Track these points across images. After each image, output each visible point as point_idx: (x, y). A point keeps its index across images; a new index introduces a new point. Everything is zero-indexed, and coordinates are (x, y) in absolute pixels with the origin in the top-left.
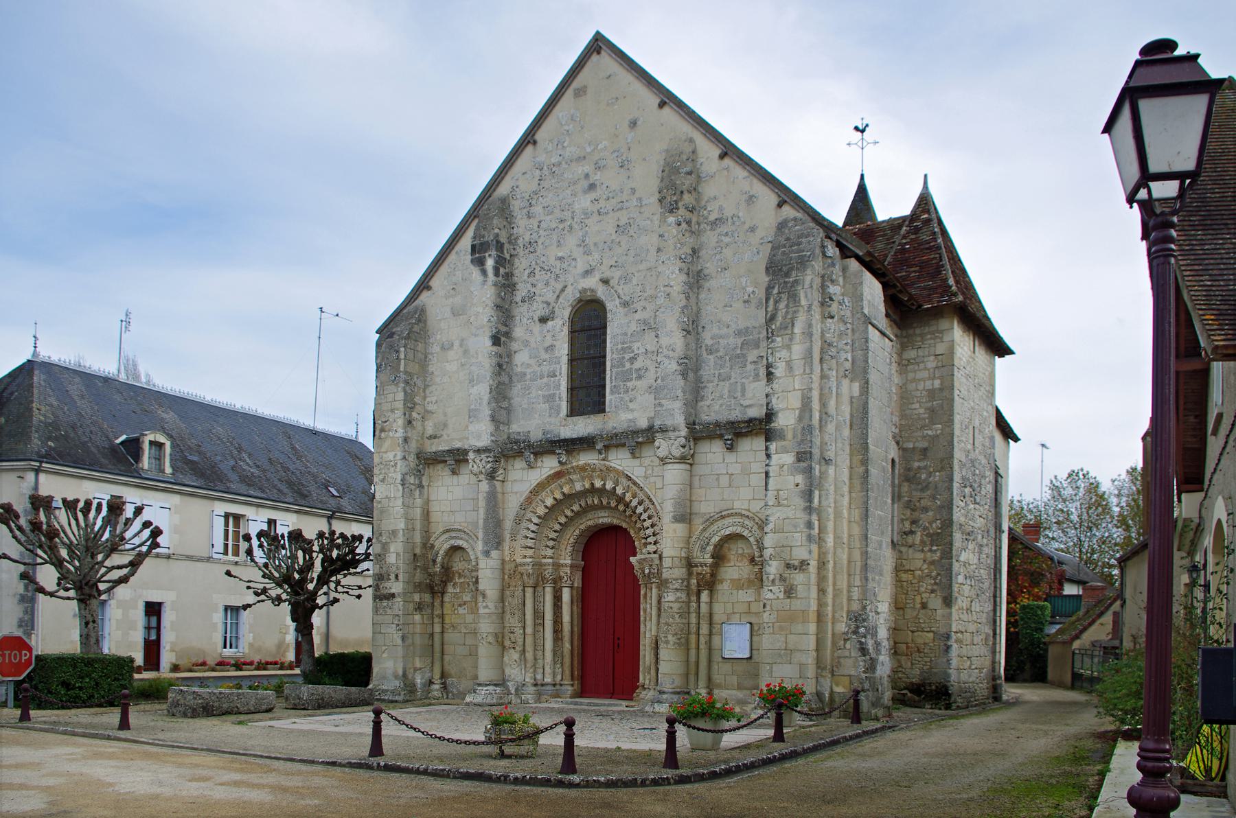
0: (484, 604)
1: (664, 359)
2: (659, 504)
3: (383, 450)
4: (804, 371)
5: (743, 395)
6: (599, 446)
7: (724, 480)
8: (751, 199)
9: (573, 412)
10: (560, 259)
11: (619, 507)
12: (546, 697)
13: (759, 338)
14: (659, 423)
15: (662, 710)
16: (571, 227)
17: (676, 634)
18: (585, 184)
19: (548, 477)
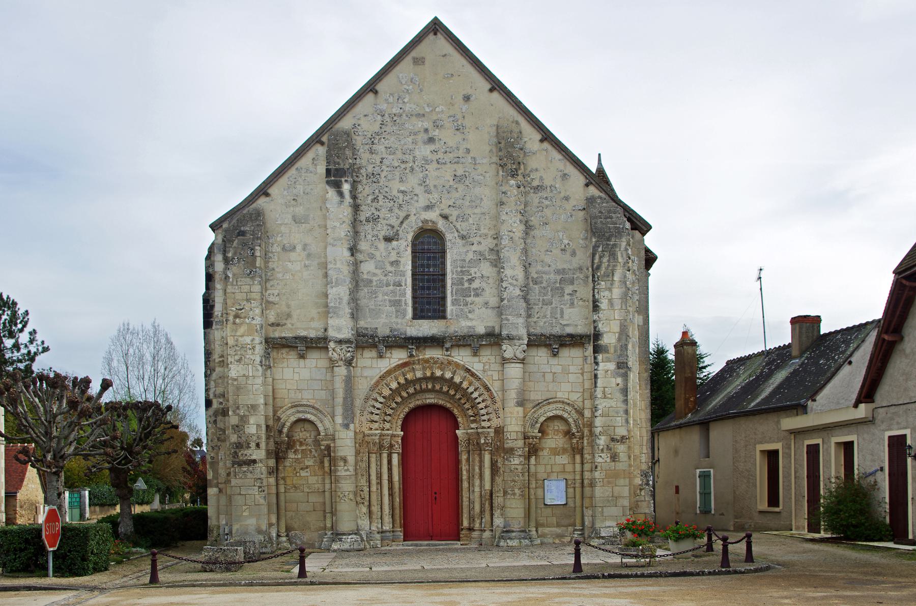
0: (346, 468)
1: (509, 285)
3: (238, 334)
4: (622, 307)
5: (562, 317)
6: (448, 345)
7: (549, 377)
8: (565, 176)
9: (416, 316)
10: (403, 192)
11: (450, 392)
12: (387, 541)
13: (573, 278)
14: (506, 333)
15: (514, 544)
16: (412, 169)
17: (520, 488)
18: (426, 137)
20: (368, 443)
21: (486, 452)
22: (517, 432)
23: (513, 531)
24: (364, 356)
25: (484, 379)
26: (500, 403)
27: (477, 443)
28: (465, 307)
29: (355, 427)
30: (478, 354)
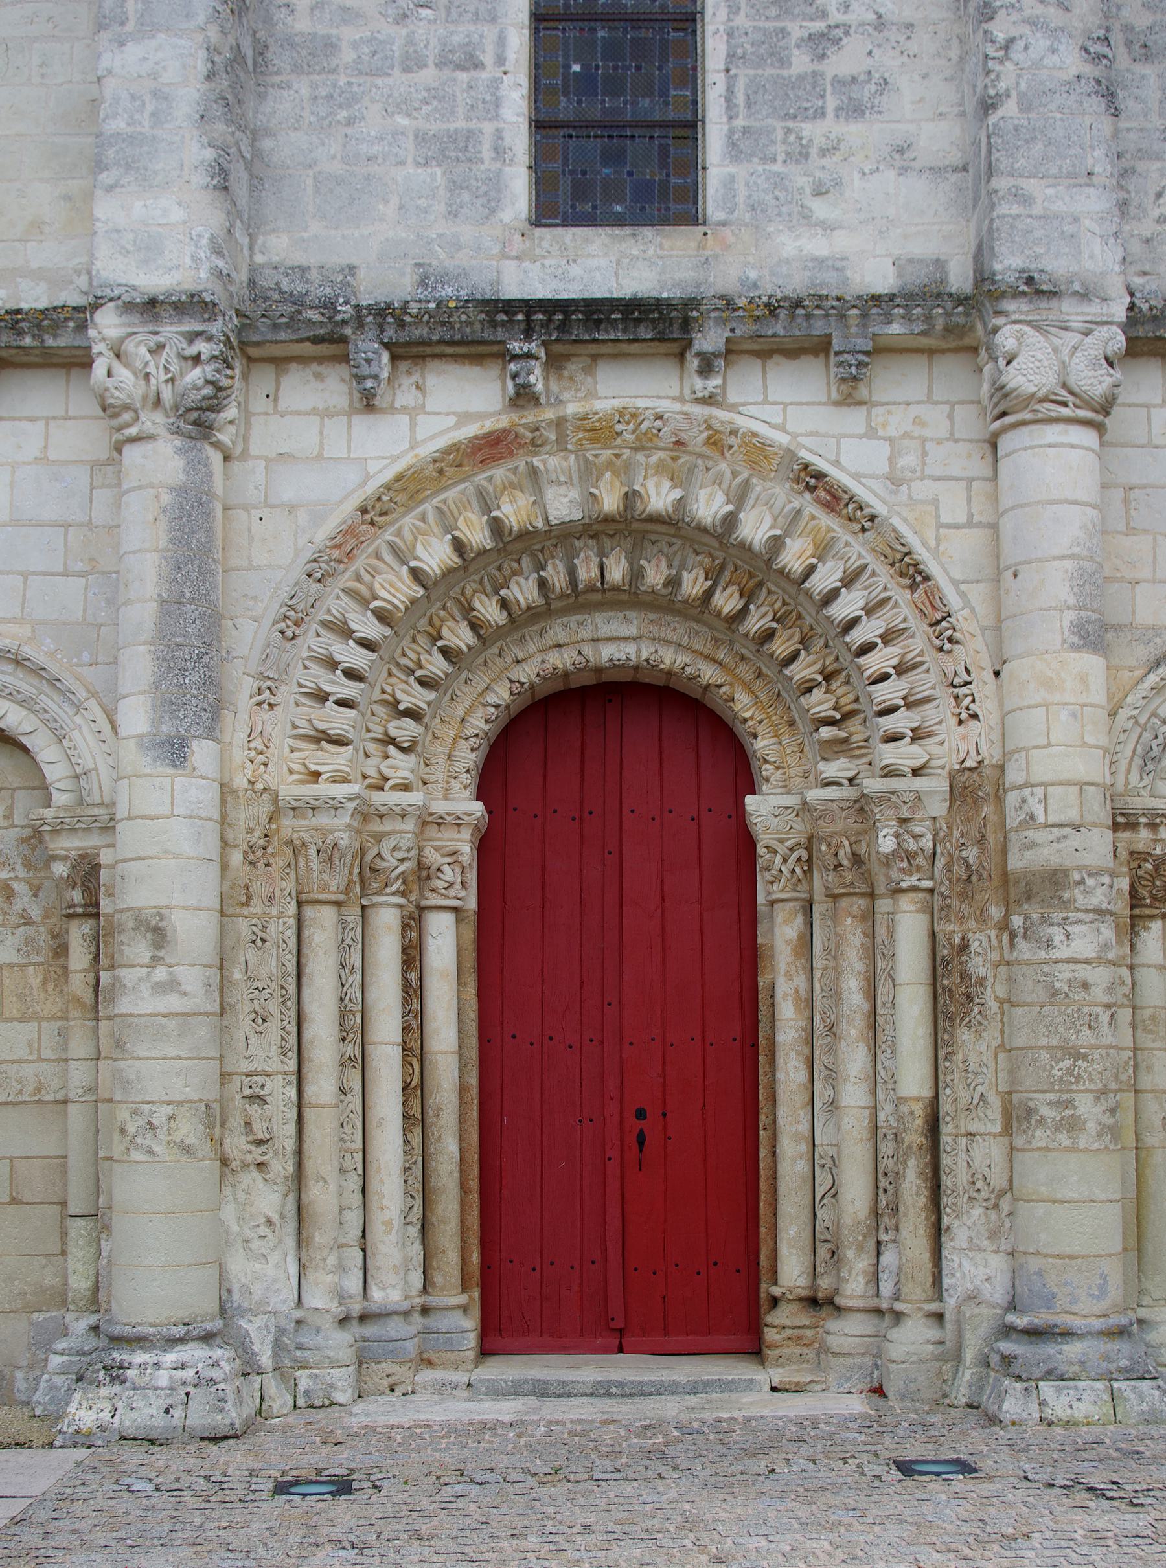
0: (161, 973)
1: (1026, 30)
2: (955, 583)
6: (710, 339)
15: (1081, 1410)
17: (1104, 1092)
19: (447, 451)
20: (297, 849)
21: (906, 903)
22: (1082, 785)
23: (1067, 1334)
24: (282, 405)
25: (896, 521)
26: (978, 643)
27: (857, 859)
28: (792, 168)
29: (223, 760)
30: (863, 391)
